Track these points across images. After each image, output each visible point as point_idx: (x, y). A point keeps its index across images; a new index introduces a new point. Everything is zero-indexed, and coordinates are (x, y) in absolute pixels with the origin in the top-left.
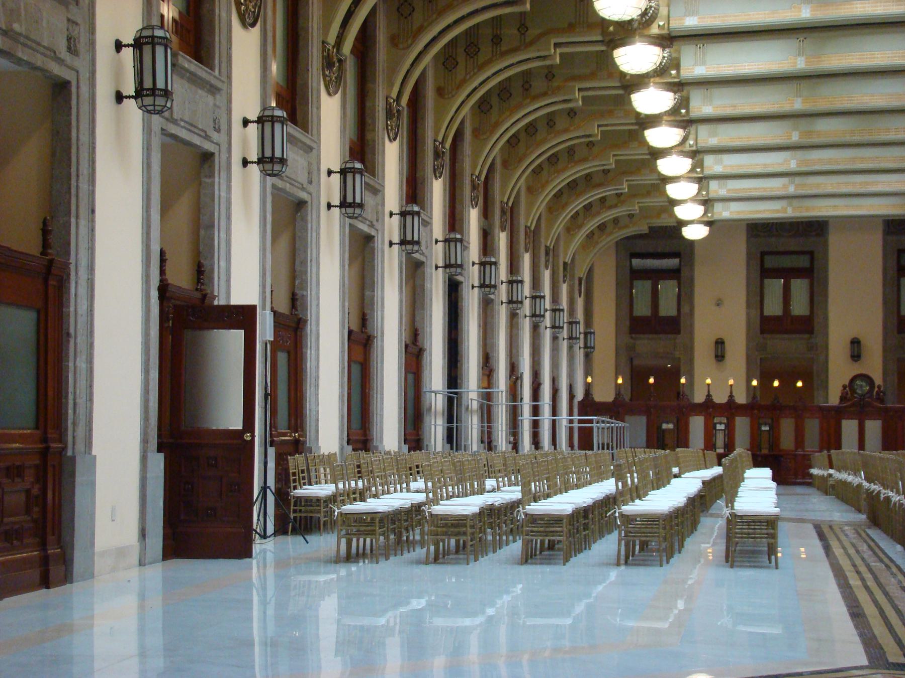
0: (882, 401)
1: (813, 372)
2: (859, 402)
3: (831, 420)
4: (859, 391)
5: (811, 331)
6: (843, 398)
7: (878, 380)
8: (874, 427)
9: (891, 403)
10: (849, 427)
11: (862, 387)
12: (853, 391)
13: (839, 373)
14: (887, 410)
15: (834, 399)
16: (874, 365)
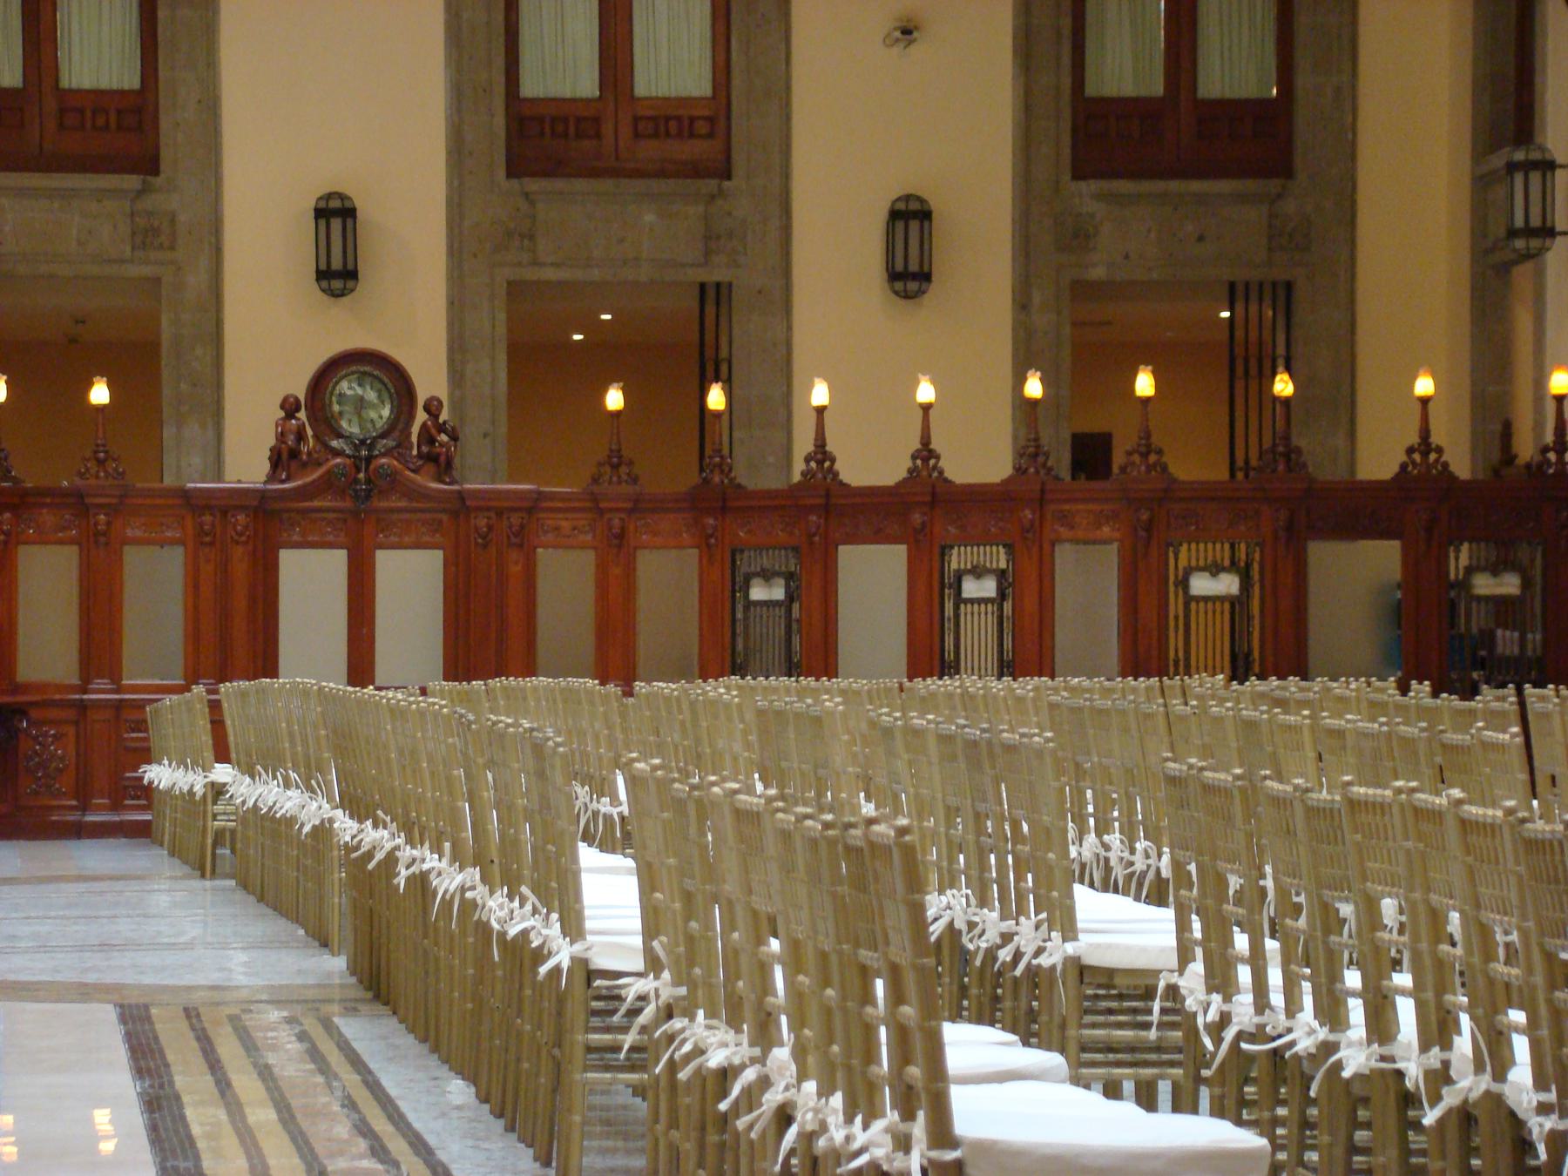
0: (441, 464)
1: (158, 348)
2: (354, 471)
3: (237, 545)
4: (350, 427)
5: (149, 164)
6: (283, 458)
7: (430, 381)
8: (411, 580)
9: (483, 472)
10: (310, 580)
11: (364, 409)
12: (325, 422)
13: (268, 344)
14: (462, 506)
15: (246, 463)
16: (412, 314)
